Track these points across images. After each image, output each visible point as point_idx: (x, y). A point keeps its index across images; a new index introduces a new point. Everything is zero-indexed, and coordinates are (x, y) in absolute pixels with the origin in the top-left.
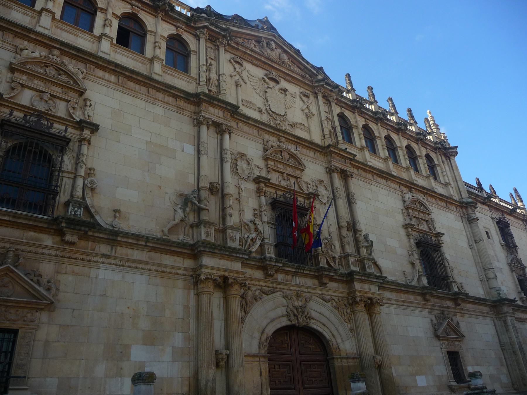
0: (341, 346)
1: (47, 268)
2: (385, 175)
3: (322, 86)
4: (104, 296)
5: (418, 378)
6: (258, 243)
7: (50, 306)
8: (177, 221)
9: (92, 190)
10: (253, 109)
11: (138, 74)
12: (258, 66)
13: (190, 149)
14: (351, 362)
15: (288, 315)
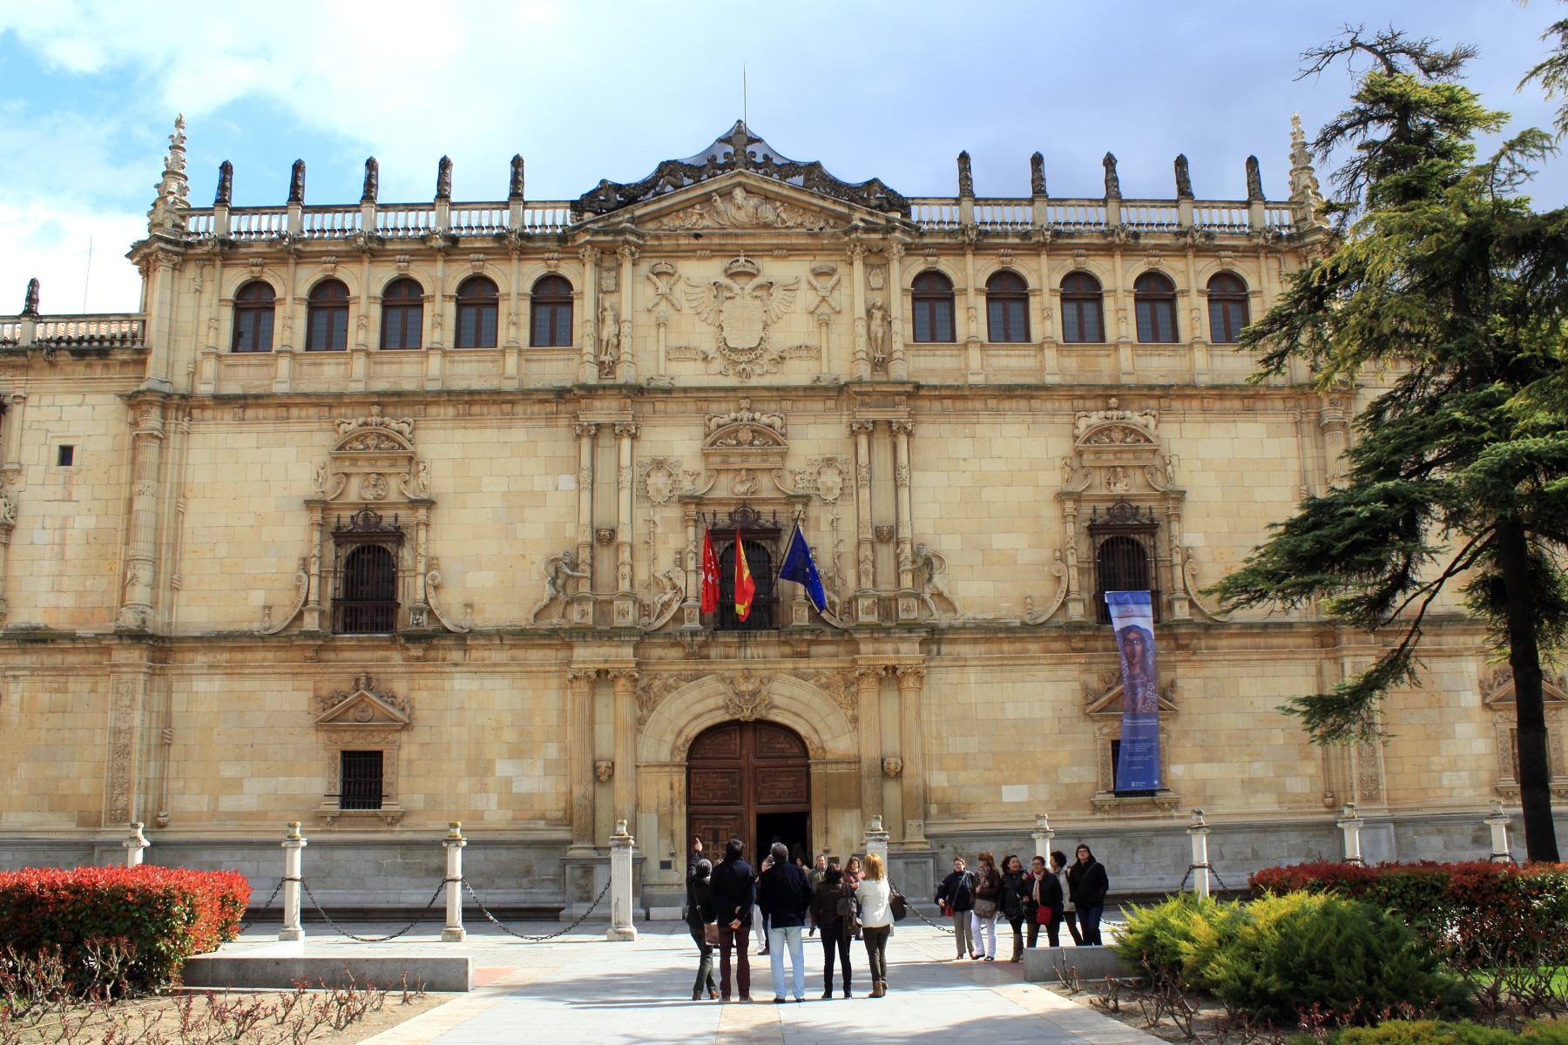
0: (829, 745)
1: (400, 687)
3: (859, 240)
4: (461, 709)
5: (1004, 788)
6: (675, 606)
7: (407, 727)
8: (546, 601)
9: (436, 587)
10: (690, 359)
11: (479, 392)
13: (567, 482)
14: (843, 769)
15: (726, 707)
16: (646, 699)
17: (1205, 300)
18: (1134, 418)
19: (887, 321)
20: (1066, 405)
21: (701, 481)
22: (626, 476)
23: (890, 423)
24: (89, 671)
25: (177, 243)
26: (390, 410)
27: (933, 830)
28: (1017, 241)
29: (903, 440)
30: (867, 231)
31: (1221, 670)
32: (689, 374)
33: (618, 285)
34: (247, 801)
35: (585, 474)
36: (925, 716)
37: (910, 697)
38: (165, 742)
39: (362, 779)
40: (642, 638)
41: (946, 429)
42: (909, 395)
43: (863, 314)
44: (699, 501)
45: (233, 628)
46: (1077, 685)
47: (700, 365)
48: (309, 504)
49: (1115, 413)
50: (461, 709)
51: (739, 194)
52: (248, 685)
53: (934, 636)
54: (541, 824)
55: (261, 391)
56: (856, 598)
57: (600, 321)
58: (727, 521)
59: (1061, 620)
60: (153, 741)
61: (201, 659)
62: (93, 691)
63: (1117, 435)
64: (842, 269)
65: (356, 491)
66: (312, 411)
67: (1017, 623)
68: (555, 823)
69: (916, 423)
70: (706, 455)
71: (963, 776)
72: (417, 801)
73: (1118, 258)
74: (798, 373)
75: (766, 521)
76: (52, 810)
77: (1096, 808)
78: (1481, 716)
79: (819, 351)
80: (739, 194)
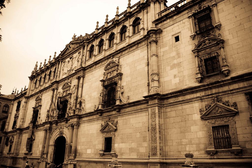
2: (98, 63)
5: (88, 150)
28: (101, 33)
31: (127, 117)
48: (33, 108)
53: (80, 117)
78: (200, 123)
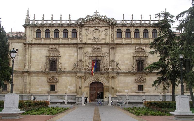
0: (106, 85)
1: (57, 77)
5: (126, 90)
7: (58, 82)
9: (61, 66)
12: (93, 27)
13: (76, 54)
15: (94, 80)
16: (85, 80)
17: (152, 33)
18: (143, 47)
19: (114, 35)
20: (134, 46)
21: (92, 54)
22: (83, 54)
23: (114, 48)
24: (21, 76)
25: (30, 25)
26: (55, 45)
27: (117, 95)
29: (115, 50)
30: (111, 24)
32: (90, 42)
33: (82, 31)
34: (40, 90)
35: (78, 53)
36: (117, 81)
37: (115, 80)
38: (30, 84)
39: (53, 88)
40: (85, 73)
41: (120, 48)
42: (116, 44)
43: (111, 35)
44: (91, 57)
45: (37, 71)
46: (134, 79)
47: (92, 41)
48: (46, 57)
49: (140, 47)
50: (64, 80)
51: (96, 19)
52: (40, 77)
53: (118, 73)
54: (73, 93)
55: (40, 43)
56: (109, 68)
57: (80, 35)
58: (94, 59)
59: (132, 71)
60: (29, 83)
61: (34, 74)
62: (21, 78)
63: (140, 49)
64: (108, 29)
65: (51, 55)
66: (46, 45)
67: (128, 71)
68: (74, 93)
69: (117, 48)
70: (92, 51)
71: (121, 88)
72: (59, 90)
73: (142, 28)
74: (103, 42)
75: (99, 59)
76: (17, 91)
77: (136, 92)
79: (105, 39)
80: (96, 19)
